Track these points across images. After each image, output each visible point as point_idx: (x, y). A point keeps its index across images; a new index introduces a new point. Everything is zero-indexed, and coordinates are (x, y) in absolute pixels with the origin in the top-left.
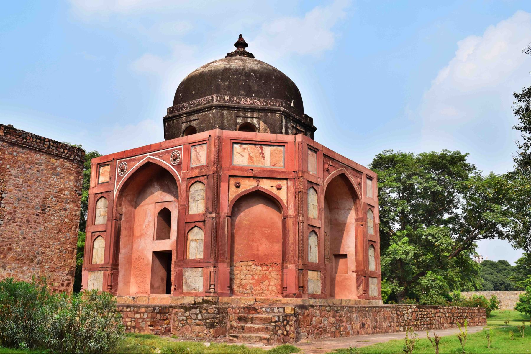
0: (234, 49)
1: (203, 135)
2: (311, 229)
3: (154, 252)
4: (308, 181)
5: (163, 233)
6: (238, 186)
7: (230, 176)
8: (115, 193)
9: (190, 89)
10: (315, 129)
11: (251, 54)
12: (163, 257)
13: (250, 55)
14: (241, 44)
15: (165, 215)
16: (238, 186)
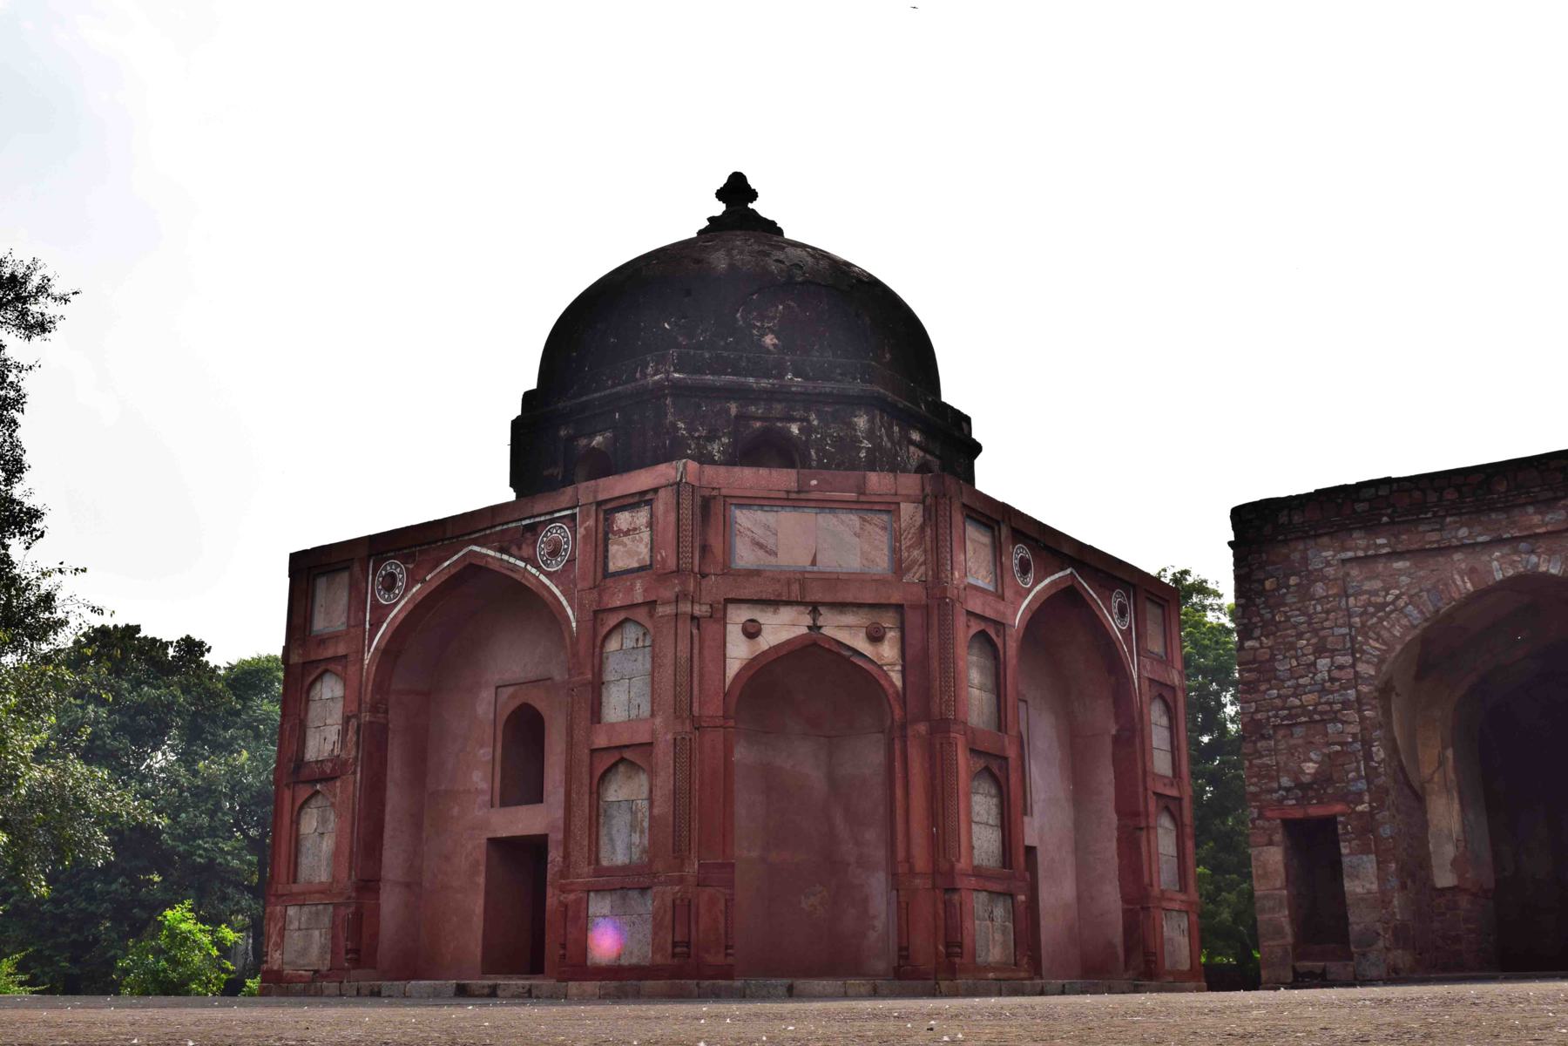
0: (719, 208)
1: (642, 480)
2: (980, 763)
3: (489, 840)
4: (969, 613)
5: (522, 784)
6: (752, 631)
7: (728, 601)
8: (367, 658)
9: (594, 333)
10: (976, 449)
11: (773, 223)
12: (522, 859)
13: (772, 228)
14: (737, 190)
15: (524, 732)
16: (752, 631)
